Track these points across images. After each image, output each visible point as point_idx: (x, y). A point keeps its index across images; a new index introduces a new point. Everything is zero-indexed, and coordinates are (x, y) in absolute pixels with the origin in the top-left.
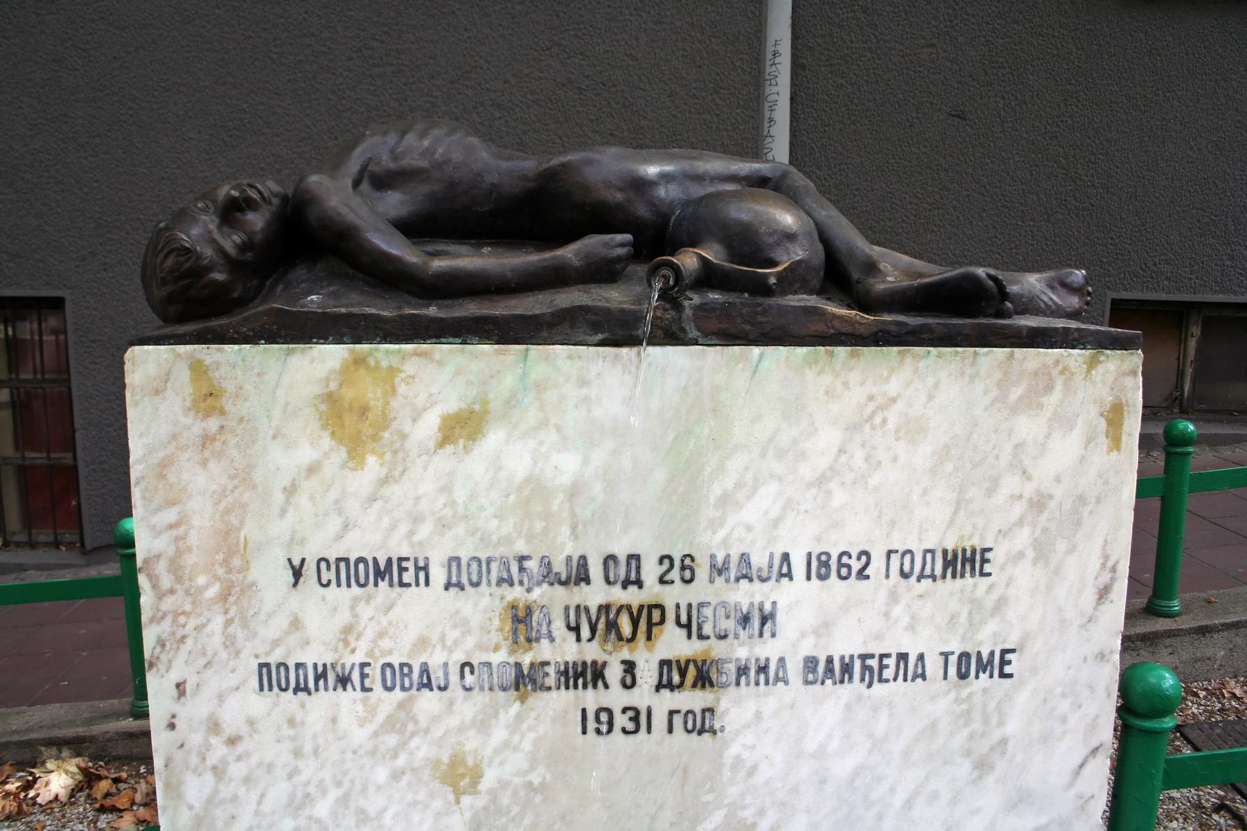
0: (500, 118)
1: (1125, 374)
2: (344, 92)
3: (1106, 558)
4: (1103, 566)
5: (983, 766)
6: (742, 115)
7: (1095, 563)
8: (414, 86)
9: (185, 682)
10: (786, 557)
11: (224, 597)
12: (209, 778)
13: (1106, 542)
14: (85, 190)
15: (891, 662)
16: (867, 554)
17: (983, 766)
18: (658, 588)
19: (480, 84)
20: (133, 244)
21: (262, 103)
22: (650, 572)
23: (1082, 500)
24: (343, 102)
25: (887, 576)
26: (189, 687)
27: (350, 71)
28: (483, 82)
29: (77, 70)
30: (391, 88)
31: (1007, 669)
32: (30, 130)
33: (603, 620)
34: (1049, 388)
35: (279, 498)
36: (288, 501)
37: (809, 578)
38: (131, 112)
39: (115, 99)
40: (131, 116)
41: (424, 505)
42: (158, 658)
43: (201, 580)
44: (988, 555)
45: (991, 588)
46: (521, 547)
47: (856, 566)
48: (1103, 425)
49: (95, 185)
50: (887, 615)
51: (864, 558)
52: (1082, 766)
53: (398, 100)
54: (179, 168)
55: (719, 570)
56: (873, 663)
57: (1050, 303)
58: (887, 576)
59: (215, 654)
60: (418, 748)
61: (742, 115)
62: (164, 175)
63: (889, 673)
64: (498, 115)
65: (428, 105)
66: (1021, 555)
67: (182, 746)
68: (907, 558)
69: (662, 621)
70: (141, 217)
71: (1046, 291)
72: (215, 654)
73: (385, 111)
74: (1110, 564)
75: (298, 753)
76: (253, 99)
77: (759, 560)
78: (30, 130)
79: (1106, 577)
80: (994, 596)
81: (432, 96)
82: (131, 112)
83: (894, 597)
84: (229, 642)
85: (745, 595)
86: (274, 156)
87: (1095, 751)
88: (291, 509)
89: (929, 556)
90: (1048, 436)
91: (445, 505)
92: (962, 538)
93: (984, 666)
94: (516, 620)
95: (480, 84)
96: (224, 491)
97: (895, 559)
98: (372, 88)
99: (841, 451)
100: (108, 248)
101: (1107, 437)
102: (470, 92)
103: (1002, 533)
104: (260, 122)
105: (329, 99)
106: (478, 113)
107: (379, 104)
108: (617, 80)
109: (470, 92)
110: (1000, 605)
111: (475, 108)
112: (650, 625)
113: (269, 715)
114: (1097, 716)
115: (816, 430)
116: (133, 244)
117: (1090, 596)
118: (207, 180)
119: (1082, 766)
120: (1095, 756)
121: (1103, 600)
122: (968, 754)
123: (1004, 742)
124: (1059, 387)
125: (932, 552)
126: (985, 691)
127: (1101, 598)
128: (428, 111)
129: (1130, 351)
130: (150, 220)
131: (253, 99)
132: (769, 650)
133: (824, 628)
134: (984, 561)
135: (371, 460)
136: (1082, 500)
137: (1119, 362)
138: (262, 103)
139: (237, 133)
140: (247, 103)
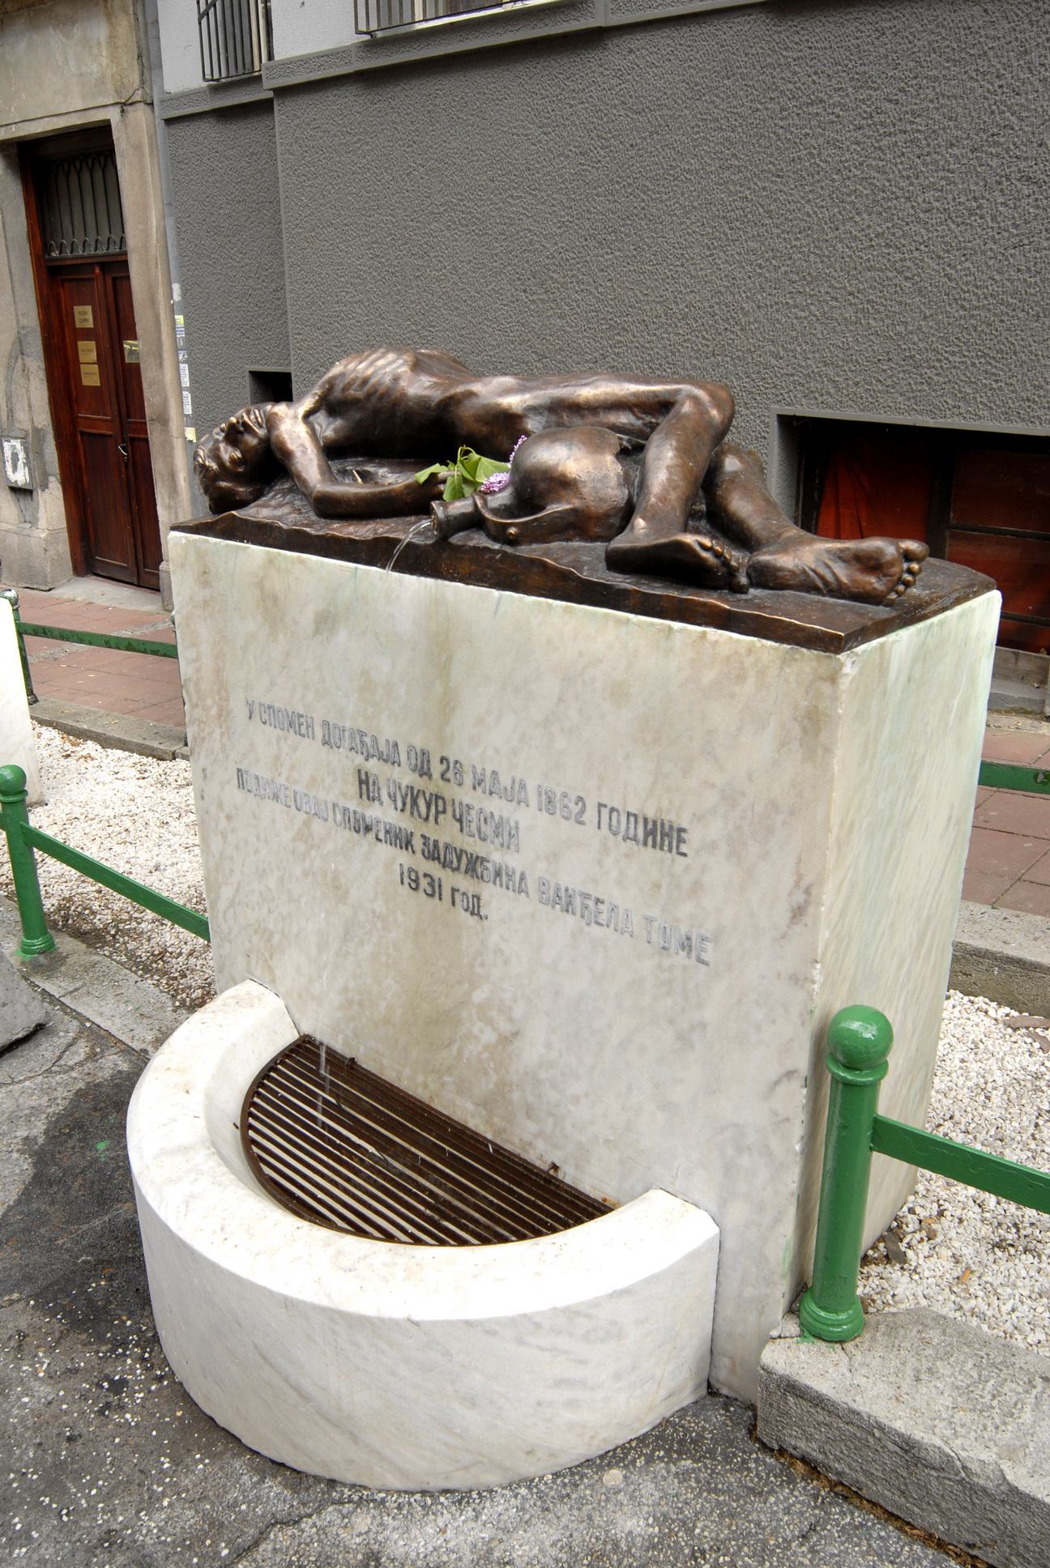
0: (1029, 196)
1: (822, 679)
2: (850, 171)
3: (800, 877)
4: (797, 884)
5: (684, 1040)
7: (788, 879)
8: (928, 159)
10: (523, 786)
11: (219, 716)
13: (799, 861)
14: (600, 289)
16: (580, 799)
17: (684, 1040)
18: (441, 782)
19: (1008, 150)
20: (637, 347)
21: (764, 189)
23: (774, 806)
24: (848, 183)
25: (599, 827)
27: (858, 143)
28: (1012, 147)
29: (600, 161)
30: (902, 163)
31: (704, 956)
32: (559, 228)
33: (409, 797)
34: (741, 678)
38: (643, 204)
39: (629, 191)
40: (643, 209)
43: (209, 702)
44: (683, 835)
45: (687, 868)
46: (361, 724)
47: (575, 809)
48: (796, 730)
49: (609, 284)
50: (600, 862)
51: (580, 804)
52: (777, 1083)
53: (908, 177)
54: (682, 265)
55: (478, 783)
57: (829, 577)
58: (599, 827)
62: (669, 274)
64: (1026, 192)
65: (943, 183)
66: (713, 846)
68: (615, 814)
69: (444, 812)
70: (646, 318)
71: (830, 563)
73: (892, 193)
74: (804, 884)
76: (755, 184)
77: (505, 780)
78: (559, 228)
79: (799, 897)
81: (948, 170)
82: (643, 204)
83: (605, 850)
84: (223, 749)
85: (496, 806)
86: (773, 250)
89: (632, 819)
90: (739, 729)
92: (659, 810)
93: (686, 945)
94: (361, 782)
95: (1008, 150)
97: (605, 812)
98: (881, 164)
99: (560, 700)
100: (617, 350)
101: (801, 745)
102: (994, 163)
103: (699, 818)
104: (761, 210)
105: (833, 180)
106: (1002, 191)
107: (887, 184)
109: (994, 163)
110: (697, 888)
111: (999, 183)
112: (437, 812)
114: (791, 1040)
116: (637, 347)
117: (782, 914)
118: (706, 279)
120: (789, 1080)
121: (796, 920)
122: (671, 1022)
124: (751, 680)
125: (635, 816)
126: (685, 968)
127: (794, 917)
128: (941, 191)
129: (828, 654)
130: (654, 323)
131: (755, 184)
132: (513, 861)
133: (553, 857)
134: (680, 841)
135: (281, 637)
136: (774, 806)
137: (814, 664)
138: (764, 189)
139: (738, 224)
140: (750, 189)
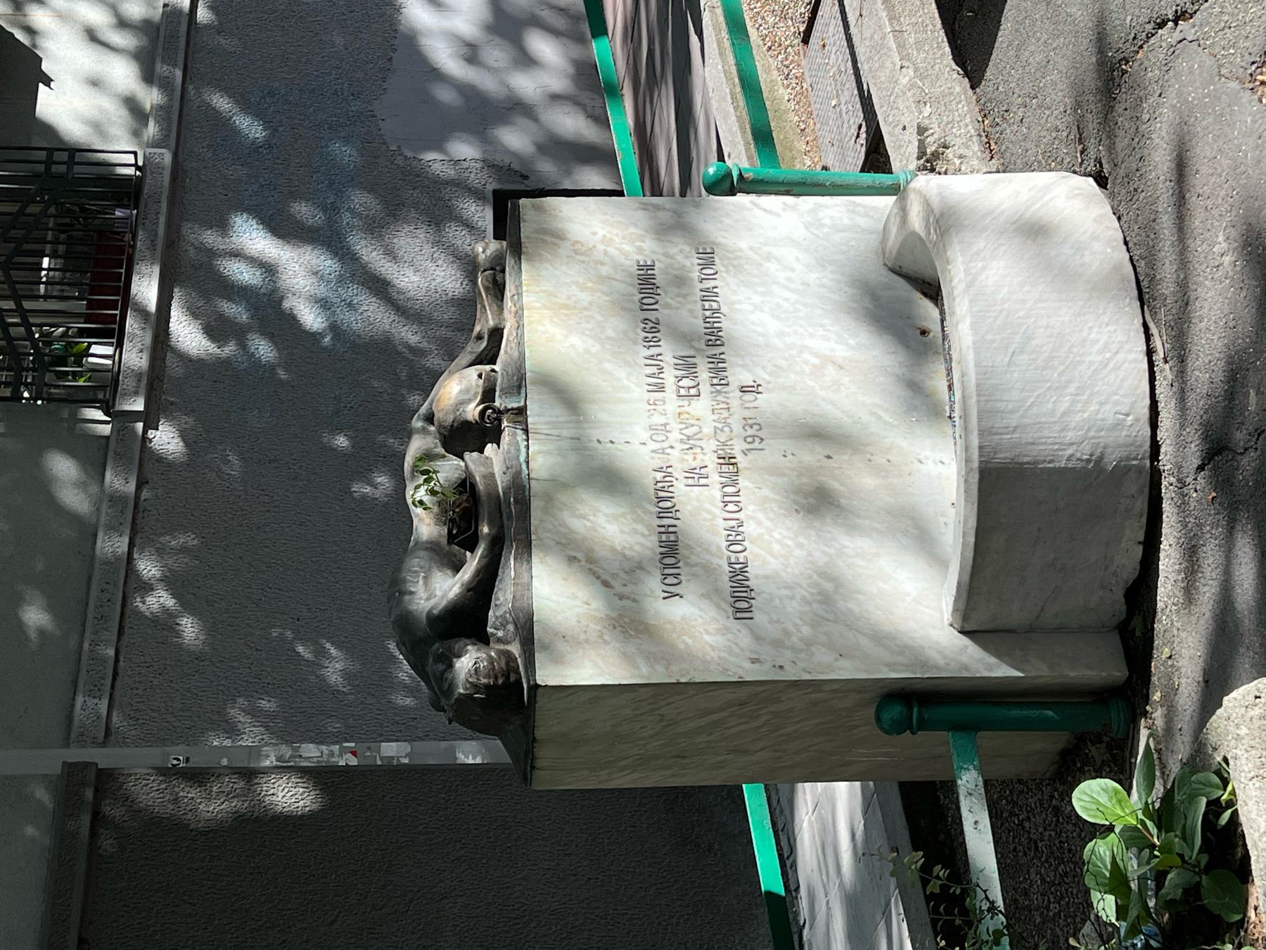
6: (286, 790)
9: (750, 659)
12: (814, 649)
15: (707, 305)
22: (658, 419)
26: (756, 656)
35: (626, 603)
36: (628, 598)
37: (659, 346)
41: (626, 529)
42: (735, 673)
45: (659, 261)
52: (765, 210)
56: (708, 313)
59: (729, 640)
60: (780, 533)
61: (286, 790)
63: (715, 305)
67: (794, 662)
72: (729, 640)
75: (792, 598)
80: (663, 258)
83: (668, 306)
87: (755, 205)
88: (632, 596)
91: (625, 518)
96: (623, 632)
108: (237, 937)
113: (767, 613)
115: (572, 345)
119: (765, 210)
123: (751, 248)
